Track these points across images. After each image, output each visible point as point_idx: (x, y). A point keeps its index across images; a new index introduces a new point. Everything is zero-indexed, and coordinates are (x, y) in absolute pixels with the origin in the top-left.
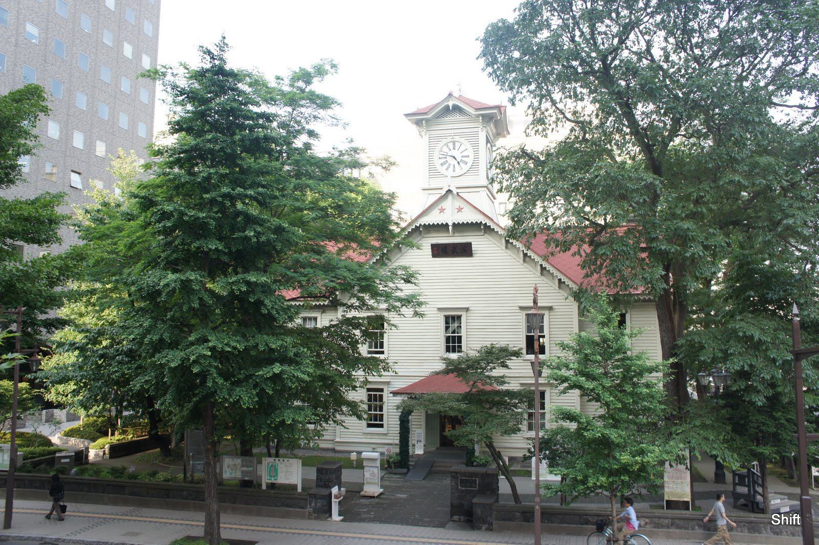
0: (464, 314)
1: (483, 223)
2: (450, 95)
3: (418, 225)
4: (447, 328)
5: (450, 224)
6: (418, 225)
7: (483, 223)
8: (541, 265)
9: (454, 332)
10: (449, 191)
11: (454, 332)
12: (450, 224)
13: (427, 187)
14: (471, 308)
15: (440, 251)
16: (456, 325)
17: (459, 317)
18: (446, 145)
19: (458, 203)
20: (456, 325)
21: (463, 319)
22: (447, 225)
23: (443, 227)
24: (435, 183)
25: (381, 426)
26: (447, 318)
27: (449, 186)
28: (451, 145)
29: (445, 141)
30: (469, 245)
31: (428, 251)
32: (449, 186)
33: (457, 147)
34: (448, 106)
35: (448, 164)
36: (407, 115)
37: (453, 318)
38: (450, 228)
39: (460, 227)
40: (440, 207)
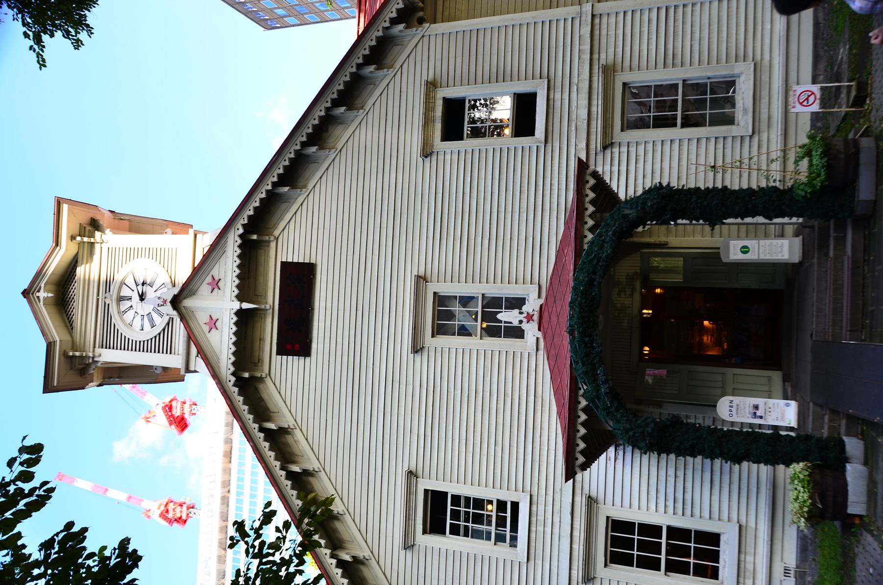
0: (432, 288)
2: (26, 293)
3: (233, 379)
4: (464, 331)
5: (236, 305)
6: (233, 379)
10: (176, 302)
12: (236, 305)
14: (422, 273)
16: (457, 308)
17: (440, 300)
18: (122, 313)
19: (205, 289)
20: (457, 308)
21: (446, 289)
22: (240, 313)
25: (515, 506)
26: (439, 330)
28: (125, 305)
29: (116, 319)
30: (287, 268)
35: (153, 313)
38: (246, 306)
40: (206, 328)
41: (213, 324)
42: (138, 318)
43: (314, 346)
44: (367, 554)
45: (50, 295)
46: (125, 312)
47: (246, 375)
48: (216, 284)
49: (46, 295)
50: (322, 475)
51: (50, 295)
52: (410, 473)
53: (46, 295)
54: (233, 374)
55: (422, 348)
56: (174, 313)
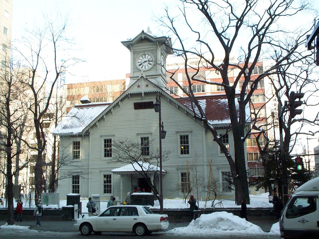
0: (150, 136)
1: (159, 91)
2: (143, 32)
3: (127, 94)
5: (143, 93)
6: (127, 94)
7: (159, 91)
8: (186, 111)
9: (145, 145)
11: (145, 145)
12: (143, 93)
13: (132, 76)
15: (138, 106)
17: (148, 138)
23: (139, 94)
24: (136, 75)
27: (142, 75)
28: (144, 57)
31: (133, 106)
32: (142, 75)
33: (146, 58)
34: (141, 37)
36: (122, 42)
37: (145, 138)
38: (143, 95)
39: (146, 94)
41: (139, 86)
42: (141, 61)
43: (137, 110)
44: (98, 128)
45: (143, 38)
46: (142, 57)
47: (129, 96)
48: (147, 86)
49: (143, 37)
50: (112, 116)
51: (143, 38)
52: (114, 135)
53: (143, 37)
54: (129, 94)
55: (138, 135)
56: (140, 77)
